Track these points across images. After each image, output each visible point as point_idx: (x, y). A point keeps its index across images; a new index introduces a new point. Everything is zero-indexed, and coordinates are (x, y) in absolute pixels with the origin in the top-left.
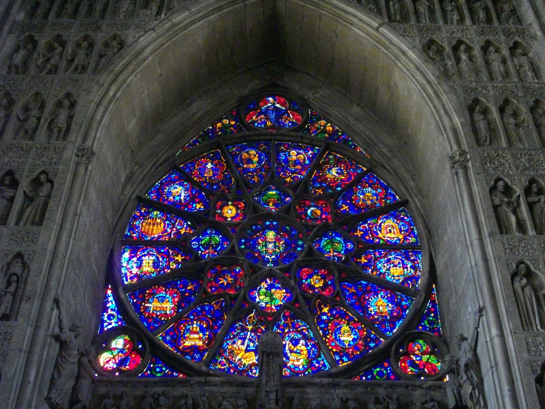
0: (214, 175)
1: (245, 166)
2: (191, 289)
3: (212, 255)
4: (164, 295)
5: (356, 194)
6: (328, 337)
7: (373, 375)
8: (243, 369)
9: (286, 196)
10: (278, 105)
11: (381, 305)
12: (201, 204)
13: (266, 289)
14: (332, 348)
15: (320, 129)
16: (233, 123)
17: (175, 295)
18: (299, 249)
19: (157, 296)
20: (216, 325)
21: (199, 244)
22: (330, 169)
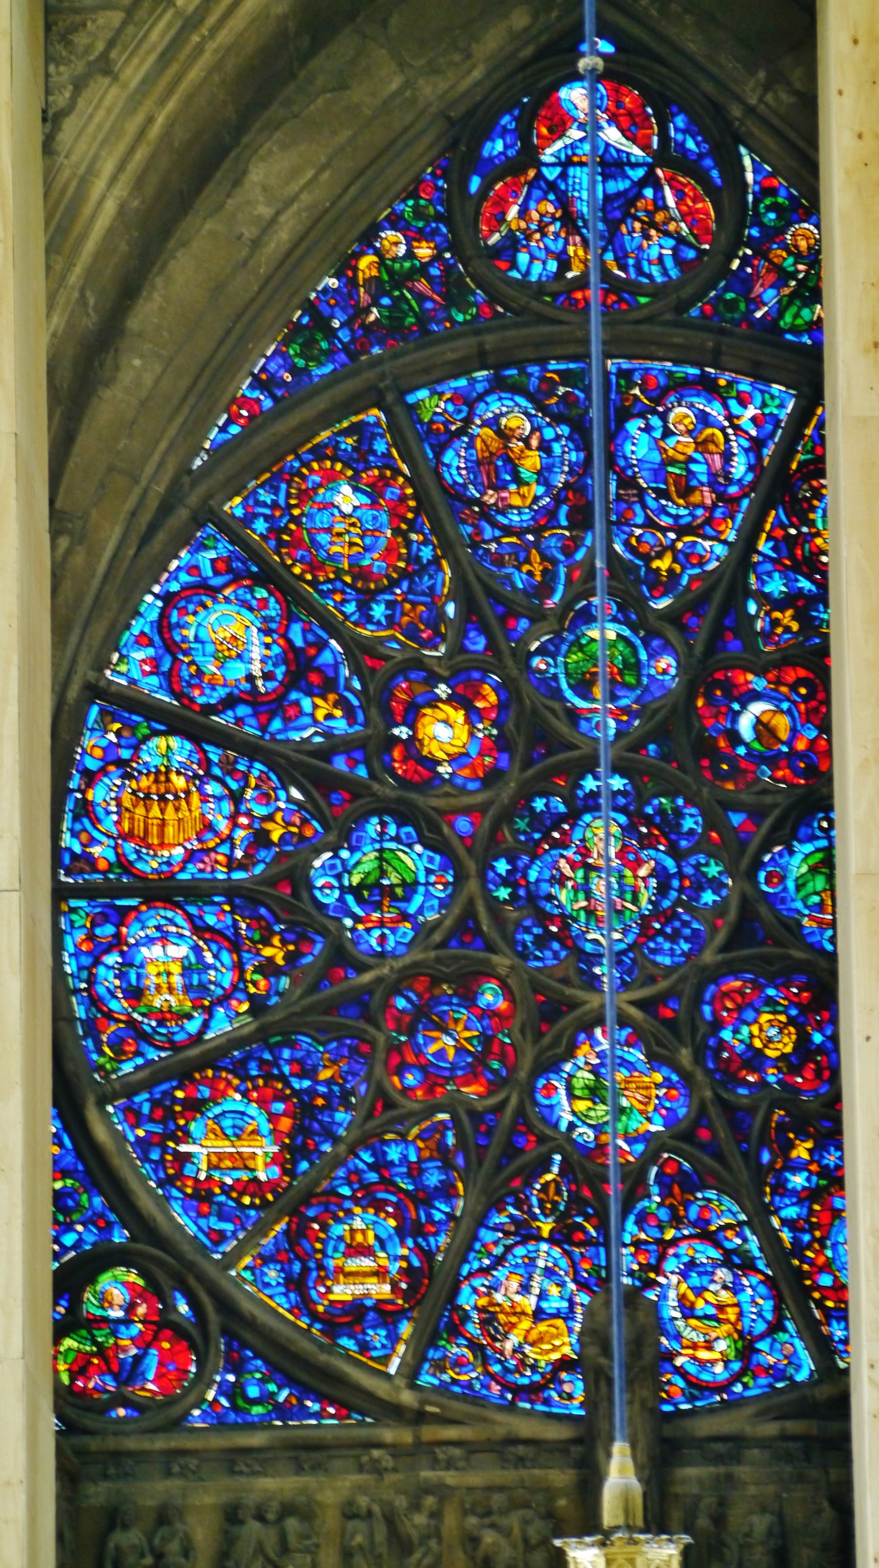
1: (490, 498)
2: (328, 1082)
3: (393, 931)
4: (241, 1108)
6: (810, 1254)
8: (533, 1383)
9: (653, 655)
10: (612, 135)
12: (332, 697)
13: (595, 1071)
14: (824, 1298)
17: (279, 1107)
18: (708, 897)
19: (217, 1110)
20: (429, 1216)
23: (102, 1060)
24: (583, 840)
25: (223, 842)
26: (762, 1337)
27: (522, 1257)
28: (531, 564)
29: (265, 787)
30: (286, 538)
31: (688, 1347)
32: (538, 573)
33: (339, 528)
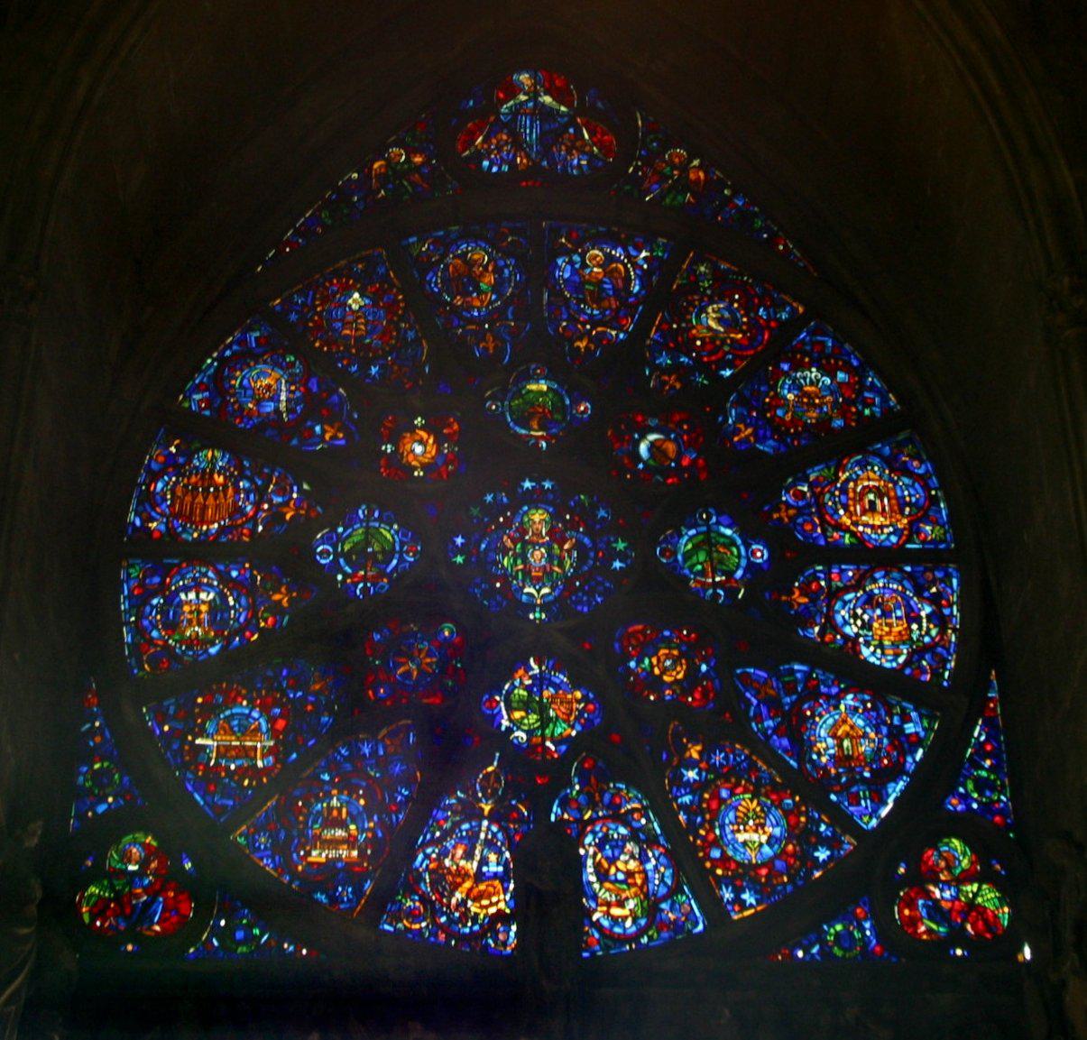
0: (368, 333)
1: (459, 301)
2: (316, 694)
3: (374, 585)
4: (247, 711)
5: (774, 387)
6: (702, 832)
7: (824, 943)
9: (575, 403)
10: (547, 99)
11: (847, 735)
13: (528, 688)
14: (714, 867)
15: (672, 176)
16: (418, 159)
17: (277, 711)
18: (617, 564)
19: (228, 713)
20: (393, 798)
21: (336, 553)
22: (703, 310)
23: (141, 674)
24: (522, 523)
25: (248, 521)
26: (664, 898)
27: (467, 831)
28: (487, 343)
29: (283, 484)
30: (311, 324)
31: (602, 905)
32: (491, 348)
33: (350, 318)
